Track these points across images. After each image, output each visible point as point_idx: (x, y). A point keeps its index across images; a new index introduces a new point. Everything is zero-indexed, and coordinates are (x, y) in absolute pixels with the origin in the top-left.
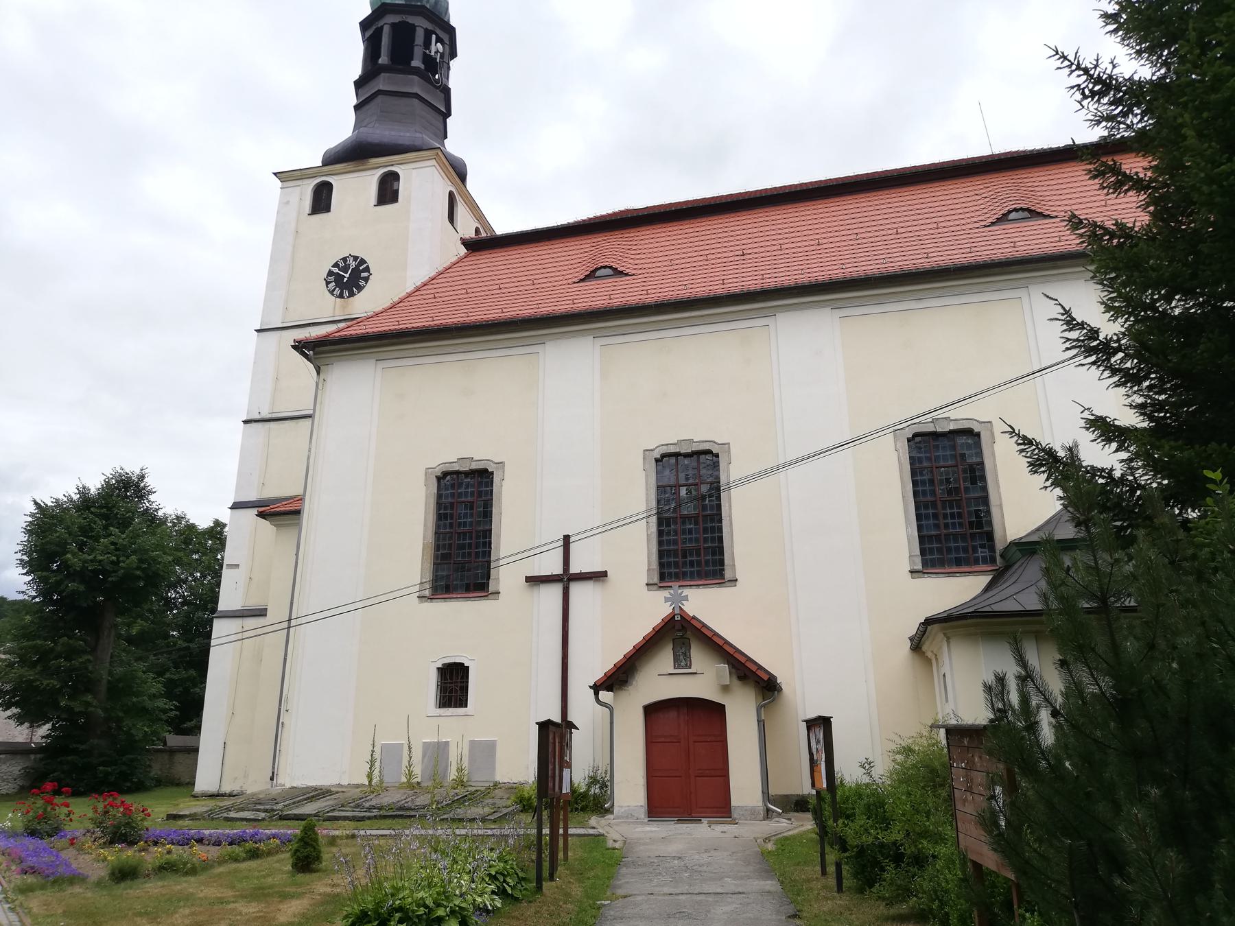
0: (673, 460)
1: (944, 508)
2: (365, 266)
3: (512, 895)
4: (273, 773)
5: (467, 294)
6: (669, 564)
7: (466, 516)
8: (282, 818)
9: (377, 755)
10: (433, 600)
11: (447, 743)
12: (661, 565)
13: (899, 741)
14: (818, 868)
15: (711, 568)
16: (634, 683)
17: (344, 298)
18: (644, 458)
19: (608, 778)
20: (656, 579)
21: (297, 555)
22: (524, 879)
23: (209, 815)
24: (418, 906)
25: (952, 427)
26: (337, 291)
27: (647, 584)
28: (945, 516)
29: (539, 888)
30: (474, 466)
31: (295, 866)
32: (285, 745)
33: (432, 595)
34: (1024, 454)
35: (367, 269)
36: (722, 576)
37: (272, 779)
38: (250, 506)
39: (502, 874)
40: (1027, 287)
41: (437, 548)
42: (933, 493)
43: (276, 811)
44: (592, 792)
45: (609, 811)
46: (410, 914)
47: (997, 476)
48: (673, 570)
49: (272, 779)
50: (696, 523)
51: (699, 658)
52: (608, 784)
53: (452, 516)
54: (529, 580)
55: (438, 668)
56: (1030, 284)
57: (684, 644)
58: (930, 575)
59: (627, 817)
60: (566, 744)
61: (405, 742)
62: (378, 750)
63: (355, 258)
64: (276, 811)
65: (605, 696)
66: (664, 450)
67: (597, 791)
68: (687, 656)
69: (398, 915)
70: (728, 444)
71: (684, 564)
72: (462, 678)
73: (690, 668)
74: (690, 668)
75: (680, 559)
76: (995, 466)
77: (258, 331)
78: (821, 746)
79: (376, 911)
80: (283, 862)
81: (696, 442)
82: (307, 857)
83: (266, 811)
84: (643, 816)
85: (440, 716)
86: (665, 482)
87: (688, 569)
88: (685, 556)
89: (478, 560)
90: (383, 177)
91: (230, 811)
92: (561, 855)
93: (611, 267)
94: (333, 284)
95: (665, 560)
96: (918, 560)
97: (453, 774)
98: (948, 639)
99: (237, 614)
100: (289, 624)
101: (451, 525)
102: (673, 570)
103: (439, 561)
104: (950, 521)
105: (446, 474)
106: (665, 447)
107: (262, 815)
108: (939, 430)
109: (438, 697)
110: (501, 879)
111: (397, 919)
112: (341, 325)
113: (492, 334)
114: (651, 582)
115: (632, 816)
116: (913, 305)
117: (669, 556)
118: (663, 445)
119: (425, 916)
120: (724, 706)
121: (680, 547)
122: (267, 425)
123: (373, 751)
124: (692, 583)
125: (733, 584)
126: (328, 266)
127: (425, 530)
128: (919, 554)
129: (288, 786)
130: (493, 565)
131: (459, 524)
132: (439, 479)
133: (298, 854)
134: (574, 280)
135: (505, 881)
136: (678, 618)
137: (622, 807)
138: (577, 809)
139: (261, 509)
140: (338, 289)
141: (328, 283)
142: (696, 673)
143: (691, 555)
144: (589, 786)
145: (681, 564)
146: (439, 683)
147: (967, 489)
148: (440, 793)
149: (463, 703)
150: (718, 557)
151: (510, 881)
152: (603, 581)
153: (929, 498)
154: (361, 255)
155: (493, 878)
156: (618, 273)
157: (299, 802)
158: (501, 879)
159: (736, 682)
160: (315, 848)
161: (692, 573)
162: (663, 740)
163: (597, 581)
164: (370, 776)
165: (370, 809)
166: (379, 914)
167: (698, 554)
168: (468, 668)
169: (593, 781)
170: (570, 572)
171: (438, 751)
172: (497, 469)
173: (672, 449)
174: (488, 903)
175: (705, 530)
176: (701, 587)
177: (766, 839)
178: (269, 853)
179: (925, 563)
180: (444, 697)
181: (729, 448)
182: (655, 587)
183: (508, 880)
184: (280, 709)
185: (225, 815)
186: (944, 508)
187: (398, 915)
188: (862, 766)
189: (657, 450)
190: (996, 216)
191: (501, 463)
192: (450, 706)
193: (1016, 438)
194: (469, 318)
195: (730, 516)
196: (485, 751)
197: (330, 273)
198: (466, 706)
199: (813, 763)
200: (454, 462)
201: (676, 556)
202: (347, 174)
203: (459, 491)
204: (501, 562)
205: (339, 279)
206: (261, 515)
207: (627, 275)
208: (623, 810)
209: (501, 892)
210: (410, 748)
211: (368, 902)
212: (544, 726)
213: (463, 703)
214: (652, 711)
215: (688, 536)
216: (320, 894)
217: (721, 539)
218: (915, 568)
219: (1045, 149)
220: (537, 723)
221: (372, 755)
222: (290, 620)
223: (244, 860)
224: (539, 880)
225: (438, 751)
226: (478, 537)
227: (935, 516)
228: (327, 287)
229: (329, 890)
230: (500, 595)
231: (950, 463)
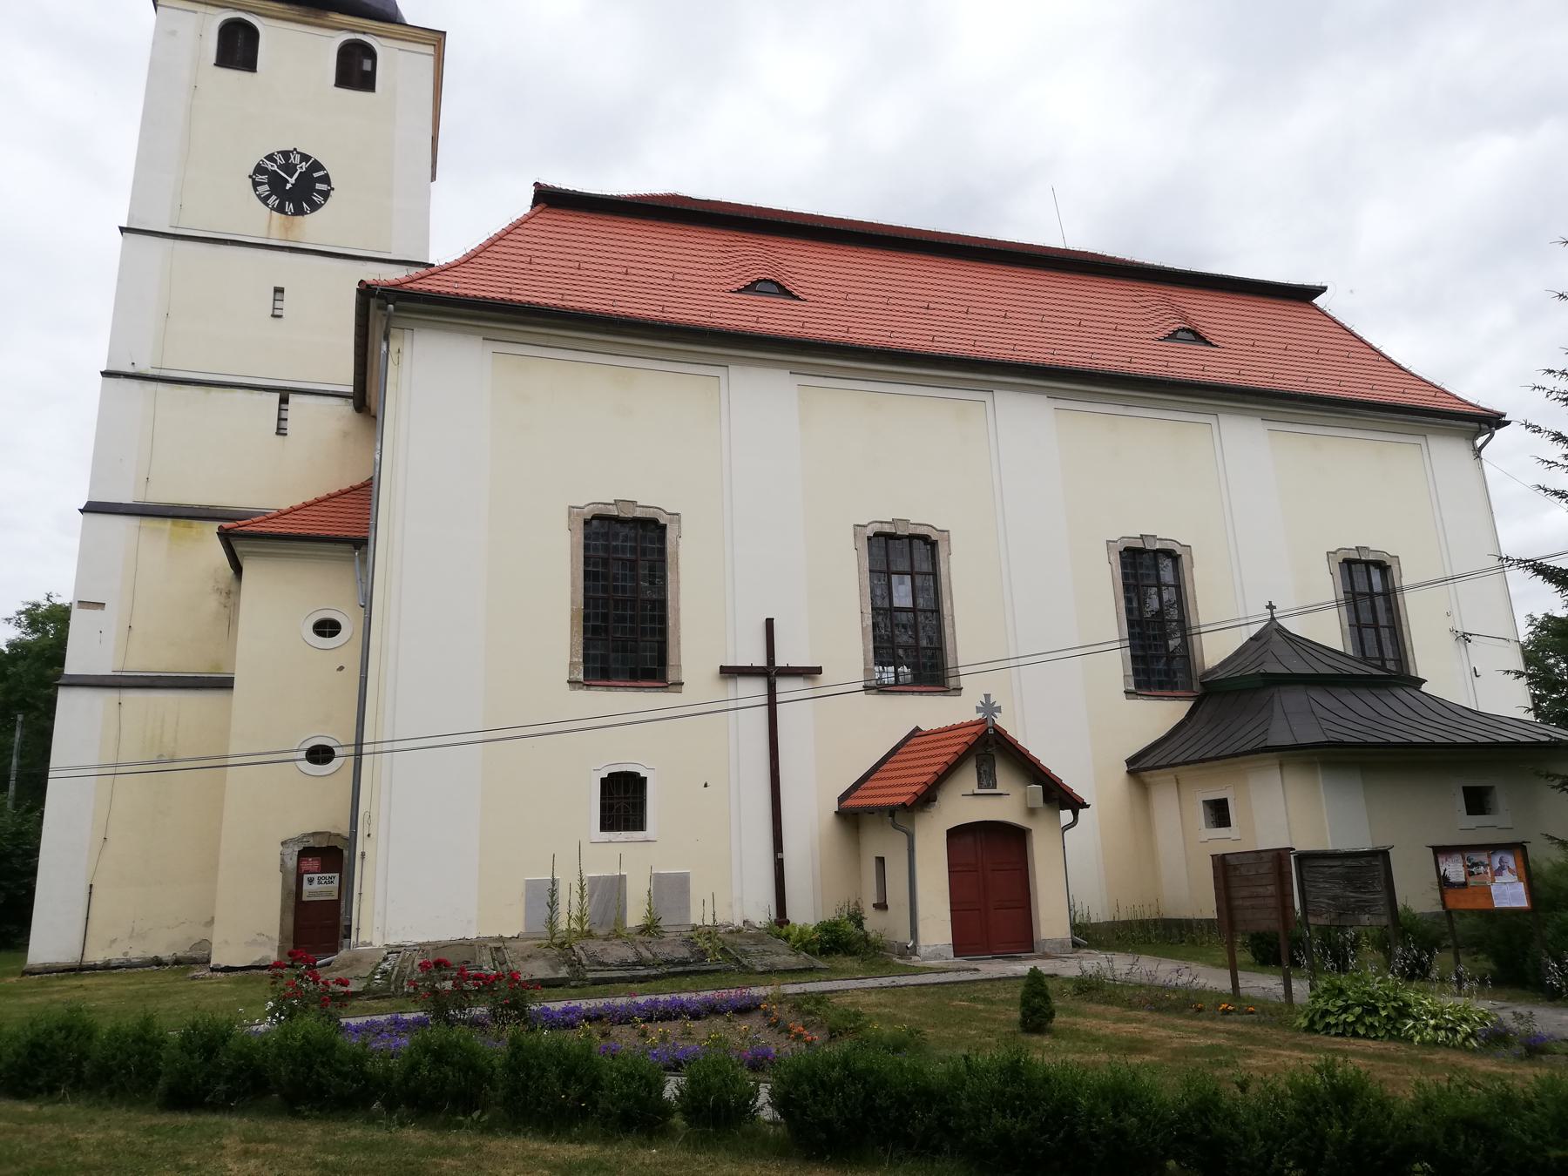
2: (322, 173)
5: (530, 263)
7: (624, 579)
17: (286, 213)
18: (855, 535)
25: (1158, 546)
26: (273, 200)
30: (638, 513)
35: (326, 179)
38: (121, 511)
40: (1425, 435)
41: (586, 618)
47: (1196, 602)
51: (1005, 779)
53: (605, 578)
56: (1221, 412)
63: (305, 158)
66: (877, 528)
70: (948, 531)
73: (994, 787)
74: (994, 787)
76: (1194, 591)
77: (122, 230)
81: (914, 524)
89: (645, 639)
90: (347, 45)
93: (777, 284)
94: (266, 187)
96: (1132, 681)
97: (635, 916)
98: (1281, 766)
99: (107, 681)
101: (605, 588)
105: (595, 517)
106: (879, 525)
112: (413, 271)
113: (607, 333)
116: (1120, 410)
118: (876, 522)
120: (948, 831)
122: (152, 386)
125: (678, 688)
126: (258, 156)
127: (573, 593)
131: (616, 588)
132: (586, 522)
134: (730, 287)
137: (928, 946)
139: (227, 525)
140: (274, 197)
141: (256, 185)
142: (1001, 794)
154: (316, 155)
156: (785, 293)
163: (809, 678)
170: (778, 664)
172: (671, 521)
173: (887, 529)
179: (1138, 684)
181: (949, 536)
190: (744, 282)
191: (677, 514)
194: (615, 309)
196: (672, 888)
197: (259, 169)
200: (609, 504)
202: (271, 20)
203: (614, 543)
205: (276, 183)
207: (797, 298)
208: (930, 950)
214: (954, 834)
218: (1129, 688)
219: (1156, 266)
228: (256, 190)
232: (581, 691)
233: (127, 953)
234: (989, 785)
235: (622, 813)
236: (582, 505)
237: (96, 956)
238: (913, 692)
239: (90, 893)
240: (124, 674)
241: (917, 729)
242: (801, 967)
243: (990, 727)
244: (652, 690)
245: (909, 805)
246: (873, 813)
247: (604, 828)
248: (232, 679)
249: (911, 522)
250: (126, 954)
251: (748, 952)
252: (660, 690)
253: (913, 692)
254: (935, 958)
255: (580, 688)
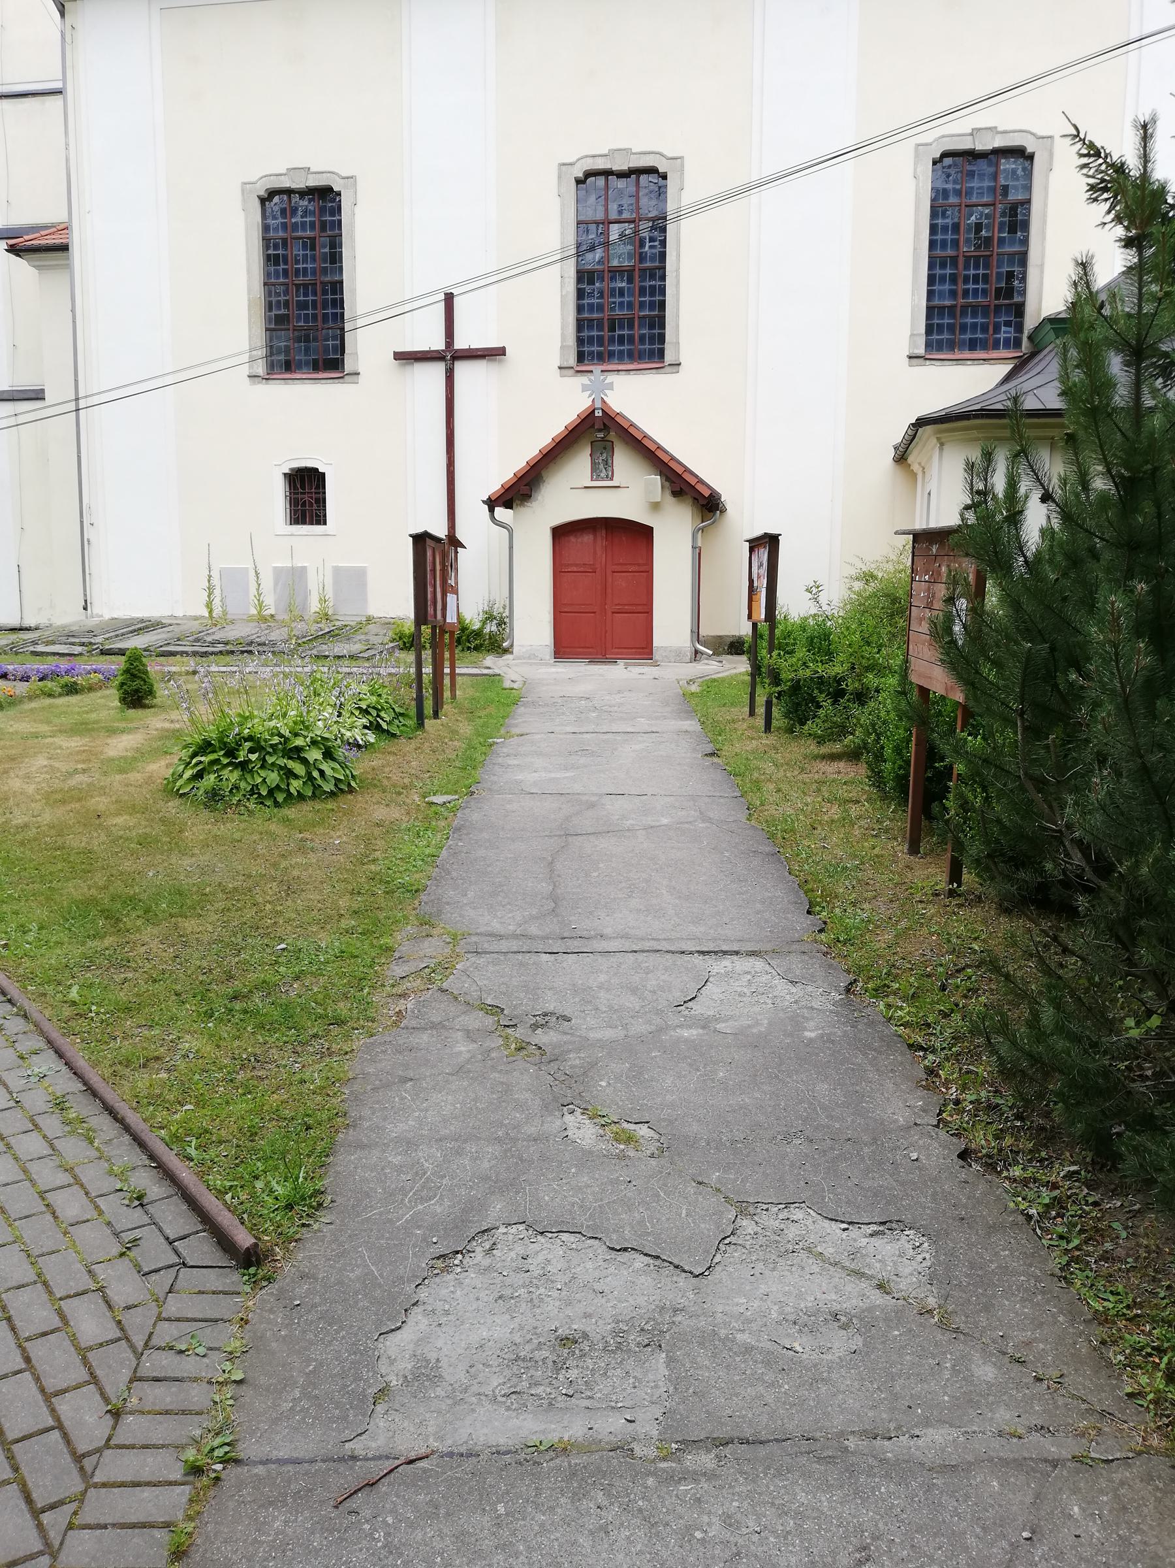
0: (601, 181)
1: (967, 267)
3: (388, 731)
4: (86, 601)
6: (591, 340)
7: (305, 261)
8: (104, 653)
9: (216, 581)
10: (270, 382)
11: (304, 569)
12: (580, 341)
13: (859, 565)
14: (747, 709)
15: (647, 346)
16: (539, 498)
18: (559, 177)
19: (507, 613)
20: (572, 360)
21: (73, 311)
22: (402, 714)
23: (11, 649)
24: (272, 735)
25: (998, 142)
28: (966, 280)
29: (420, 724)
30: (313, 182)
31: (123, 700)
32: (94, 567)
33: (268, 374)
34: (1085, 171)
36: (661, 354)
37: (85, 608)
39: (374, 708)
41: (269, 306)
42: (956, 243)
43: (95, 644)
44: (487, 630)
45: (506, 651)
46: (263, 743)
48: (595, 348)
49: (85, 608)
50: (630, 281)
52: (506, 620)
54: (400, 356)
57: (605, 448)
58: (933, 362)
59: (529, 658)
60: (449, 566)
61: (250, 566)
62: (215, 575)
64: (95, 644)
65: (501, 512)
67: (494, 628)
68: (608, 464)
69: (248, 745)
70: (681, 158)
71: (612, 340)
72: (317, 487)
75: (606, 333)
76: (1045, 205)
78: (764, 571)
79: (221, 740)
80: (110, 698)
82: (137, 691)
83: (83, 644)
84: (548, 657)
86: (589, 215)
87: (616, 348)
88: (612, 329)
91: (37, 644)
92: (447, 694)
95: (585, 334)
97: (314, 606)
100: (77, 405)
102: (595, 348)
103: (273, 326)
104: (971, 286)
105: (272, 193)
106: (590, 160)
107: (77, 649)
108: (979, 147)
109: (288, 510)
110: (374, 713)
111: (246, 749)
114: (565, 365)
115: (536, 657)
117: (590, 328)
118: (587, 156)
119: (280, 746)
121: (606, 314)
123: (210, 576)
127: (249, 280)
128: (924, 331)
129: (107, 616)
130: (347, 327)
133: (125, 687)
135: (378, 716)
136: (598, 413)
138: (469, 648)
142: (619, 487)
143: (622, 327)
144: (484, 623)
145: (606, 338)
146: (288, 494)
147: (1001, 241)
148: (300, 627)
149: (321, 519)
150: (656, 331)
151: (385, 716)
152: (500, 361)
153: (950, 252)
155: (365, 712)
157: (123, 635)
158: (374, 713)
159: (669, 499)
160: (145, 681)
161: (621, 352)
162: (575, 569)
163: (495, 360)
164: (209, 605)
165: (213, 643)
166: (225, 744)
167: (631, 327)
168: (323, 474)
169: (489, 617)
170: (456, 347)
171: (294, 578)
173: (601, 164)
174: (359, 739)
175: (642, 291)
176: (632, 373)
177: (691, 680)
178: (91, 689)
180: (296, 512)
181: (682, 165)
182: (571, 372)
183: (382, 714)
184: (82, 522)
185: (32, 649)
186: (967, 267)
187: (248, 745)
188: (809, 590)
189: (578, 165)
192: (304, 523)
193: (1079, 145)
195: (678, 270)
198: (325, 523)
199: (752, 590)
200: (281, 175)
201: (600, 328)
203: (293, 220)
204: (360, 323)
206: (13, 250)
209: (375, 727)
210: (257, 574)
211: (213, 735)
212: (421, 540)
213: (321, 519)
214: (561, 533)
215: (618, 300)
216: (157, 730)
217: (662, 305)
220: (411, 536)
221: (209, 581)
222: (77, 399)
223: (60, 695)
224: (420, 717)
225: (294, 578)
226: (325, 292)
227: (954, 279)
229: (167, 725)
231: (985, 199)
234: (607, 477)
236: (254, 179)
238: (618, 371)
243: (598, 409)
244: (329, 381)
248: (43, 391)
249: (633, 151)
252: (336, 381)
253: (618, 371)
255: (259, 383)
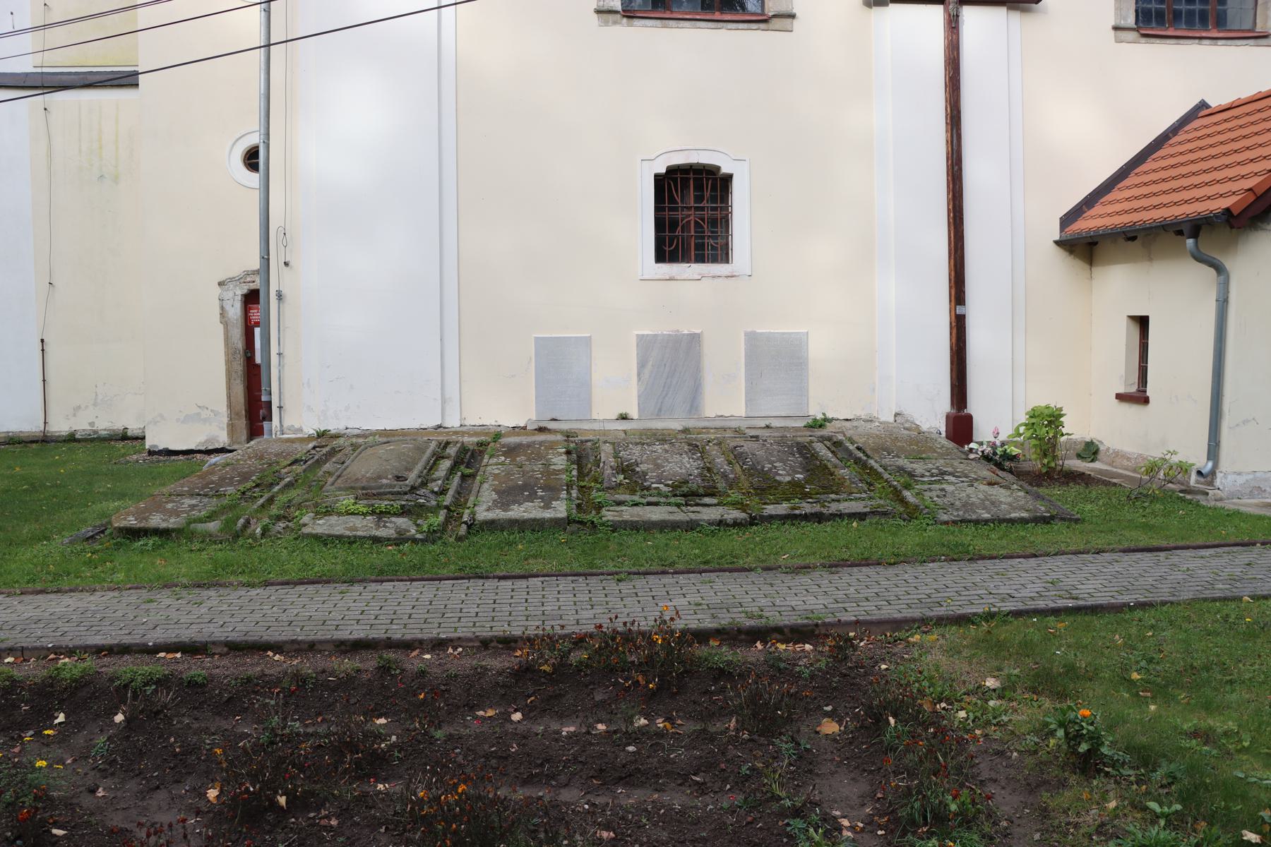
27: (1116, 28)
55: (657, 176)
85: (670, 280)
114: (1123, 23)
124: (1204, 34)
137: (1239, 474)
161: (1190, 14)
168: (728, 179)
176: (1220, 42)
230: (795, 22)
232: (617, 28)
233: (94, 423)
235: (693, 234)
237: (60, 426)
239: (43, 350)
240: (45, 70)
241: (1203, 105)
242: (1025, 515)
244: (741, 26)
245: (1235, 213)
246: (1133, 239)
247: (661, 257)
250: (92, 424)
251: (911, 475)
253: (1201, 38)
254: (1251, 495)
255: (615, 23)
